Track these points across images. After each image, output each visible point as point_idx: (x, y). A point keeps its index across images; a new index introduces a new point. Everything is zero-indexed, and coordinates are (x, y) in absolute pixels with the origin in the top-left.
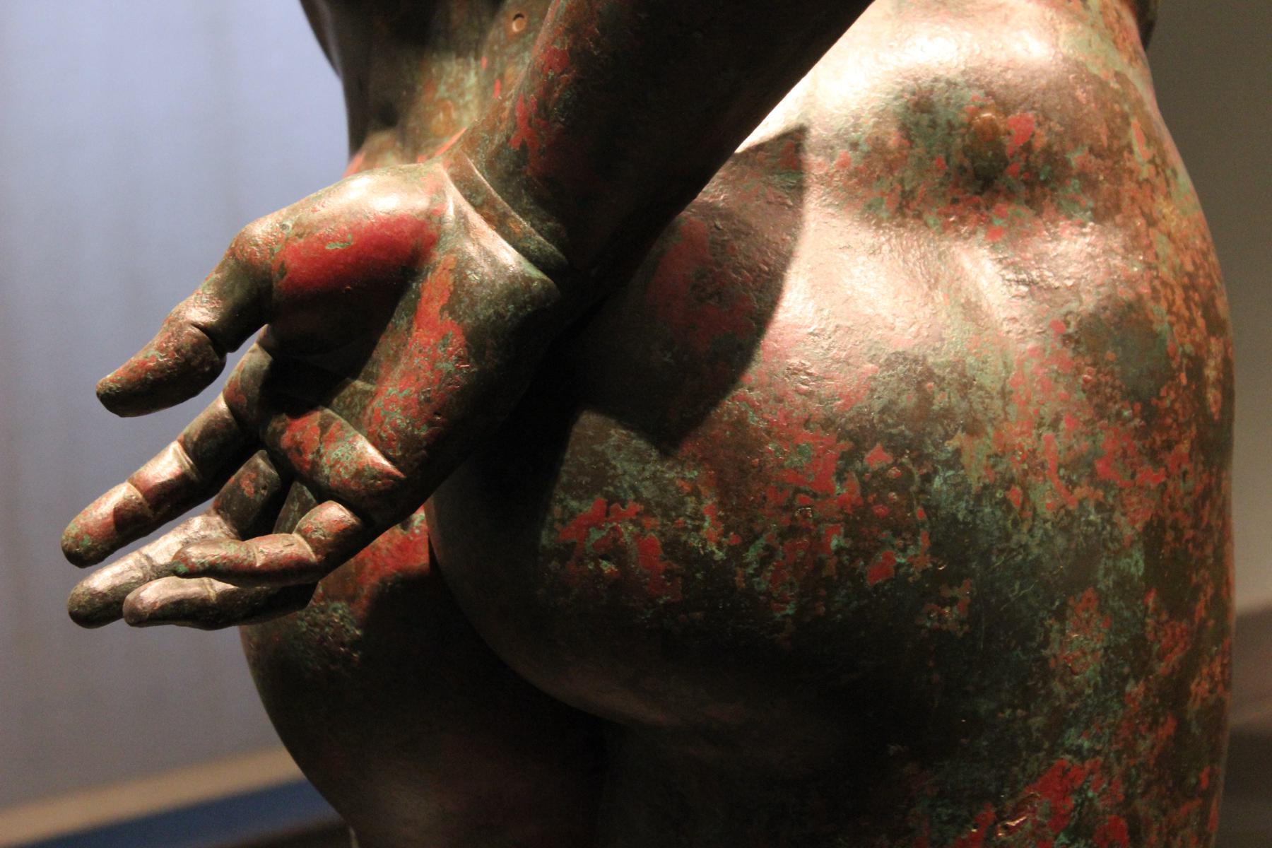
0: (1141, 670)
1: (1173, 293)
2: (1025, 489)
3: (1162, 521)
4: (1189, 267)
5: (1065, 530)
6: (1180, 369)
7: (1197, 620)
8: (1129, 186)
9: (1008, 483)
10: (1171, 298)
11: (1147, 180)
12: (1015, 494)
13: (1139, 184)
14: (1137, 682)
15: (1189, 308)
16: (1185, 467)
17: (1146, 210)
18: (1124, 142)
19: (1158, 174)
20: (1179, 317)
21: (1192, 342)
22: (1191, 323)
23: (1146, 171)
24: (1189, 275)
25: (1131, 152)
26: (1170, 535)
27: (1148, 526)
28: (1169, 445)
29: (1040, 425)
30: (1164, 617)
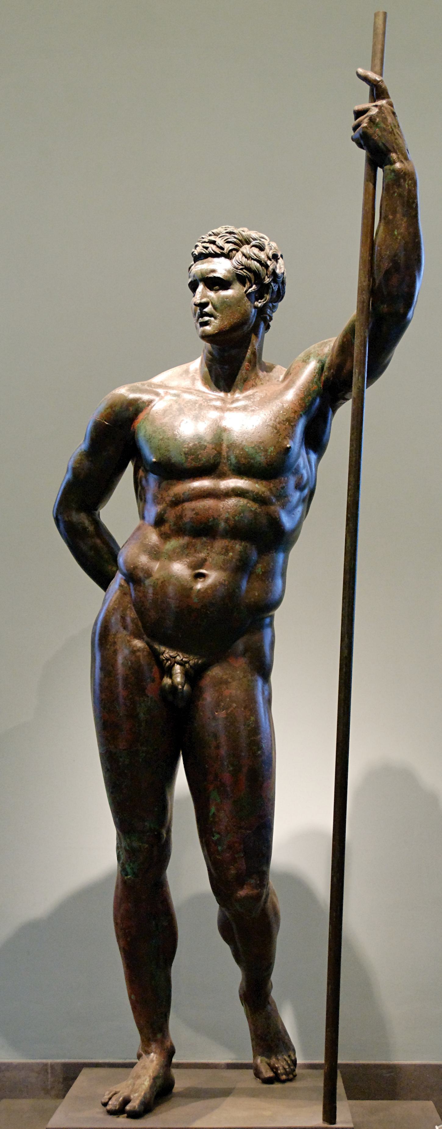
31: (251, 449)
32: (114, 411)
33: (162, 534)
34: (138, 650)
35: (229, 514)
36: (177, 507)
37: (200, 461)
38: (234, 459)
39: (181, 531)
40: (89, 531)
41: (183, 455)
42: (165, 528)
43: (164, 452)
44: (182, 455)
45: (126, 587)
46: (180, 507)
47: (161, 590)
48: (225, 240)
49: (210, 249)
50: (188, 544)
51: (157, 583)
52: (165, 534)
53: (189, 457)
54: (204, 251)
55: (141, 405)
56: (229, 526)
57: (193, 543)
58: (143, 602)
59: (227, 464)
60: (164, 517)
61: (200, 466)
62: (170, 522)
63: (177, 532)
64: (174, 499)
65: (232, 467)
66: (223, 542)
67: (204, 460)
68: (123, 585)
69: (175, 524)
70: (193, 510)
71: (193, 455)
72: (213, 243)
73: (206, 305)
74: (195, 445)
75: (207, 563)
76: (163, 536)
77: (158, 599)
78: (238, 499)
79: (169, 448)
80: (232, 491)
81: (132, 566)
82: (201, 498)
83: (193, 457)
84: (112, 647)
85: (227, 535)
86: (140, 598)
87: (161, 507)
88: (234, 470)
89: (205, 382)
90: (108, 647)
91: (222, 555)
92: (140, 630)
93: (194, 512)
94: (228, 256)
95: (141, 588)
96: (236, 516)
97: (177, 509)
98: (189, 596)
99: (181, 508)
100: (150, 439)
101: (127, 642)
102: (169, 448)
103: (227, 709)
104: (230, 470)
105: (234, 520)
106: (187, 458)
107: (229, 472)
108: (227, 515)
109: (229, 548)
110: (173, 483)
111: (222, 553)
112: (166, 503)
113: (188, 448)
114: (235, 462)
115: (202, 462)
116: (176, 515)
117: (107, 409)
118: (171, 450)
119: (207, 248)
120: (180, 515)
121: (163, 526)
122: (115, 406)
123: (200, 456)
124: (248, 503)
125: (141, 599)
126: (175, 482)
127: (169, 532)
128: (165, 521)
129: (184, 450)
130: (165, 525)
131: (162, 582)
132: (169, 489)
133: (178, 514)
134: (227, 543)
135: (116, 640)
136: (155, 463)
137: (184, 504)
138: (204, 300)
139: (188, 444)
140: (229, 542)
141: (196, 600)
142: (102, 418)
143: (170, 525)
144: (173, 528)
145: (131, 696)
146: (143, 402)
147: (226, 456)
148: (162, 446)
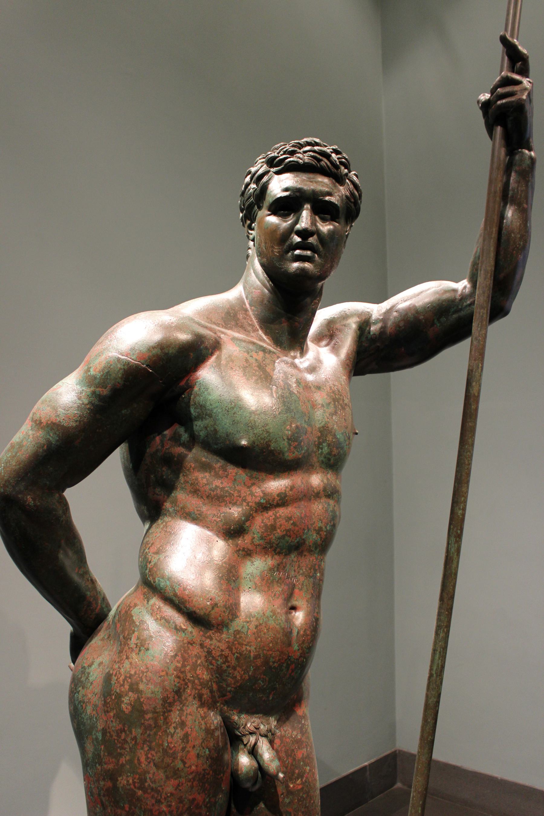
0: (100, 764)
1: (121, 676)
2: (86, 706)
3: (106, 730)
4: (133, 672)
5: (90, 719)
6: (113, 694)
7: (121, 762)
8: (127, 648)
9: (84, 702)
10: (119, 677)
11: (131, 648)
12: (84, 706)
13: (129, 648)
14: (99, 765)
15: (124, 682)
16: (112, 719)
17: (128, 655)
18: (130, 637)
19: (136, 647)
20: (118, 682)
21: (120, 690)
22: (123, 685)
23: (132, 646)
24: (131, 675)
25: (131, 640)
26: (108, 735)
27: (103, 728)
28: (108, 712)
29: (94, 693)
30: (106, 754)
31: (341, 435)
32: (166, 354)
33: (239, 550)
34: (216, 729)
35: (321, 522)
36: (267, 513)
37: (302, 450)
38: (326, 448)
39: (271, 547)
40: (62, 521)
41: (286, 440)
42: (244, 541)
43: (261, 432)
44: (284, 440)
45: (191, 632)
46: (270, 513)
47: (256, 639)
48: (338, 159)
49: (323, 163)
50: (278, 565)
51: (248, 629)
52: (244, 550)
53: (293, 443)
54: (314, 162)
55: (204, 352)
56: (321, 538)
57: (284, 564)
58: (226, 657)
59: (317, 454)
60: (245, 526)
61: (300, 456)
62: (254, 534)
63: (265, 548)
64: (262, 501)
65: (322, 458)
66: (311, 559)
67: (305, 449)
68: (186, 629)
69: (261, 538)
70: (289, 519)
71: (296, 442)
72: (327, 156)
73: (311, 234)
74: (297, 427)
75: (296, 590)
76: (240, 552)
77: (250, 651)
78: (327, 500)
79: (267, 427)
80: (323, 491)
81: (208, 603)
82: (297, 501)
83: (296, 443)
84: (179, 730)
85: (316, 548)
86: (222, 651)
87: (240, 509)
88: (323, 462)
89: (266, 331)
90: (172, 730)
91: (310, 577)
92: (214, 697)
93: (292, 522)
94: (339, 179)
95: (224, 636)
96: (327, 524)
97: (266, 515)
98: (290, 644)
99: (273, 513)
100: (233, 408)
101: (200, 719)
102: (267, 427)
103: (302, 777)
104: (318, 462)
105: (325, 530)
106: (290, 445)
107: (317, 464)
108: (320, 524)
109: (317, 568)
110: (261, 477)
111: (311, 574)
112: (248, 505)
113: (290, 430)
114: (327, 452)
115: (304, 451)
116: (266, 526)
117: (154, 348)
118: (271, 431)
119: (319, 160)
120: (272, 525)
121: (241, 539)
122: (168, 346)
123: (302, 443)
124: (335, 506)
125: (223, 653)
126: (264, 474)
127: (250, 547)
128: (245, 530)
129: (286, 432)
130: (244, 537)
131: (256, 627)
132: (253, 484)
133: (269, 524)
134: (315, 561)
135: (183, 718)
136: (243, 448)
137: (277, 509)
138: (314, 228)
139: (291, 426)
140: (317, 559)
141: (296, 647)
142: (142, 361)
143: (254, 538)
144: (257, 541)
145: (207, 800)
146: (206, 348)
147: (316, 443)
148: (257, 424)
